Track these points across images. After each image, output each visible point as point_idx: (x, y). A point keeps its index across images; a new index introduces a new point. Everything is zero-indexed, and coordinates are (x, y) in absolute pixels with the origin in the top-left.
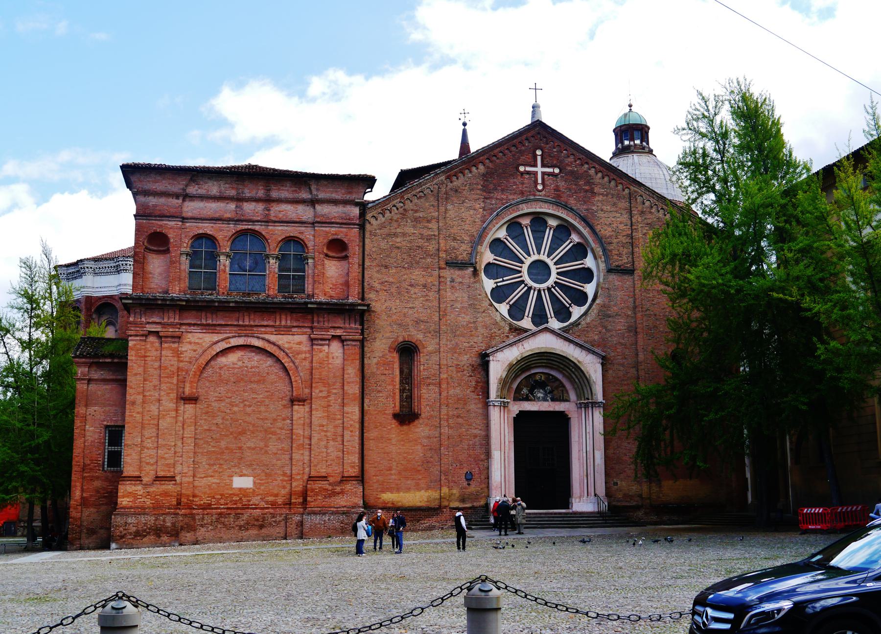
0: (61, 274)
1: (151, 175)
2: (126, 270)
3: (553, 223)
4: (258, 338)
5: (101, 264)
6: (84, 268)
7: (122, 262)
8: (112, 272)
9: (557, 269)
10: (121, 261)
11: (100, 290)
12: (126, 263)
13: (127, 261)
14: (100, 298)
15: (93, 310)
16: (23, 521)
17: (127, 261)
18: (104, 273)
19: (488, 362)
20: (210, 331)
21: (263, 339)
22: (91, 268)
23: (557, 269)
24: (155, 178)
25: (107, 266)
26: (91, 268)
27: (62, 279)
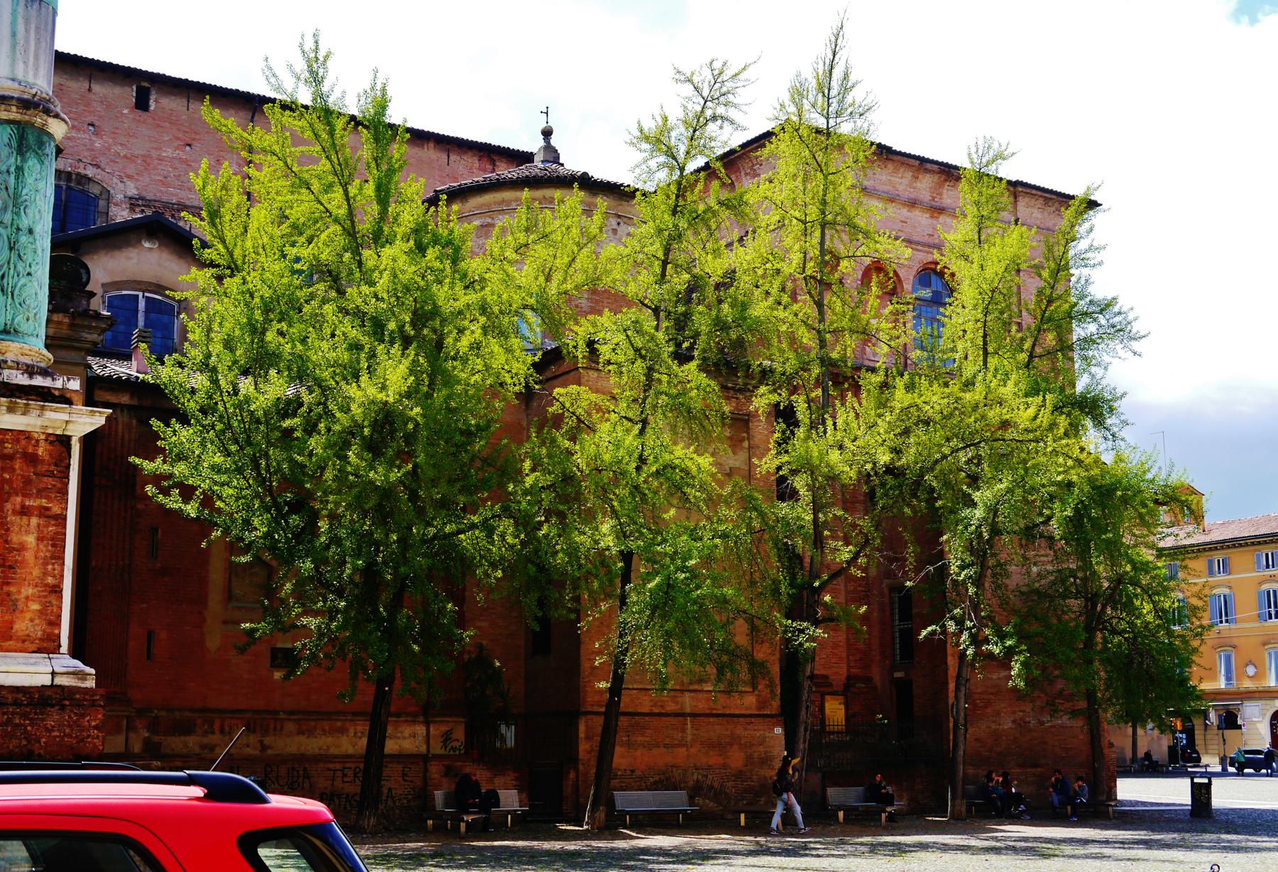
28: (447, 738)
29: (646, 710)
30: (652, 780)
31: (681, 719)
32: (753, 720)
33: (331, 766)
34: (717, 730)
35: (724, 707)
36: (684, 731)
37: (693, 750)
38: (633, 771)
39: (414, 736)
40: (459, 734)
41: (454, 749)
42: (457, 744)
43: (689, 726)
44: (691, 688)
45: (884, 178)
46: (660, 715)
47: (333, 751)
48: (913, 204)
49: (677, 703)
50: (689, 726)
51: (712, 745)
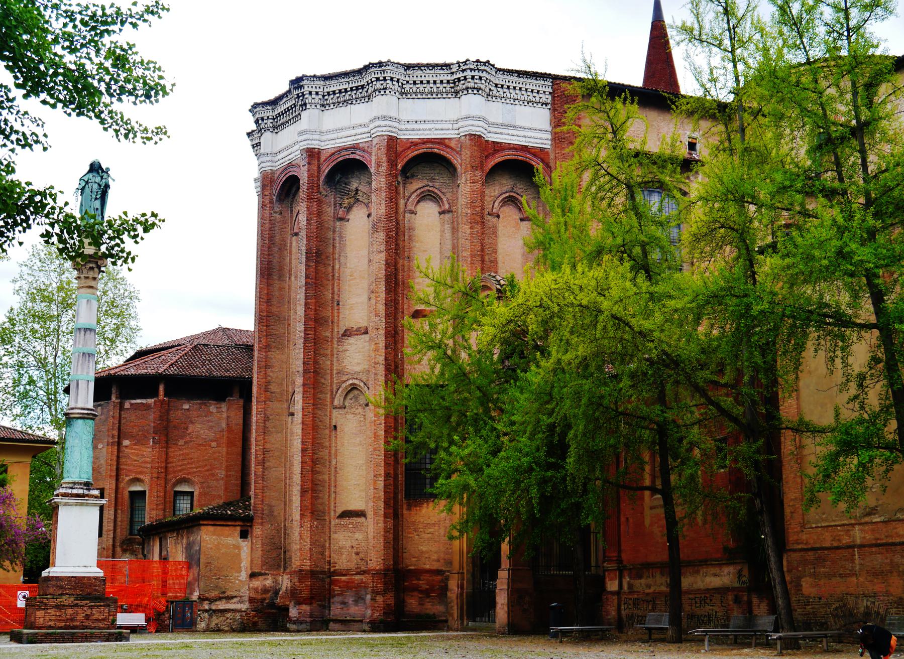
0: (310, 93)
2: (478, 89)
5: (418, 75)
6: (385, 79)
7: (473, 73)
8: (442, 93)
10: (471, 70)
11: (416, 126)
12: (480, 74)
13: (483, 71)
14: (414, 144)
15: (399, 167)
16: (207, 599)
17: (483, 71)
22: (398, 81)
25: (431, 79)
27: (311, 104)
28: (740, 574)
29: (828, 545)
30: (834, 606)
31: (850, 550)
33: (690, 596)
34: (878, 559)
35: (887, 537)
36: (853, 561)
37: (861, 579)
38: (820, 598)
39: (729, 574)
40: (745, 572)
41: (743, 583)
42: (744, 579)
43: (857, 557)
44: (863, 521)
46: (838, 548)
47: (695, 587)
49: (849, 536)
50: (857, 557)
51: (876, 574)
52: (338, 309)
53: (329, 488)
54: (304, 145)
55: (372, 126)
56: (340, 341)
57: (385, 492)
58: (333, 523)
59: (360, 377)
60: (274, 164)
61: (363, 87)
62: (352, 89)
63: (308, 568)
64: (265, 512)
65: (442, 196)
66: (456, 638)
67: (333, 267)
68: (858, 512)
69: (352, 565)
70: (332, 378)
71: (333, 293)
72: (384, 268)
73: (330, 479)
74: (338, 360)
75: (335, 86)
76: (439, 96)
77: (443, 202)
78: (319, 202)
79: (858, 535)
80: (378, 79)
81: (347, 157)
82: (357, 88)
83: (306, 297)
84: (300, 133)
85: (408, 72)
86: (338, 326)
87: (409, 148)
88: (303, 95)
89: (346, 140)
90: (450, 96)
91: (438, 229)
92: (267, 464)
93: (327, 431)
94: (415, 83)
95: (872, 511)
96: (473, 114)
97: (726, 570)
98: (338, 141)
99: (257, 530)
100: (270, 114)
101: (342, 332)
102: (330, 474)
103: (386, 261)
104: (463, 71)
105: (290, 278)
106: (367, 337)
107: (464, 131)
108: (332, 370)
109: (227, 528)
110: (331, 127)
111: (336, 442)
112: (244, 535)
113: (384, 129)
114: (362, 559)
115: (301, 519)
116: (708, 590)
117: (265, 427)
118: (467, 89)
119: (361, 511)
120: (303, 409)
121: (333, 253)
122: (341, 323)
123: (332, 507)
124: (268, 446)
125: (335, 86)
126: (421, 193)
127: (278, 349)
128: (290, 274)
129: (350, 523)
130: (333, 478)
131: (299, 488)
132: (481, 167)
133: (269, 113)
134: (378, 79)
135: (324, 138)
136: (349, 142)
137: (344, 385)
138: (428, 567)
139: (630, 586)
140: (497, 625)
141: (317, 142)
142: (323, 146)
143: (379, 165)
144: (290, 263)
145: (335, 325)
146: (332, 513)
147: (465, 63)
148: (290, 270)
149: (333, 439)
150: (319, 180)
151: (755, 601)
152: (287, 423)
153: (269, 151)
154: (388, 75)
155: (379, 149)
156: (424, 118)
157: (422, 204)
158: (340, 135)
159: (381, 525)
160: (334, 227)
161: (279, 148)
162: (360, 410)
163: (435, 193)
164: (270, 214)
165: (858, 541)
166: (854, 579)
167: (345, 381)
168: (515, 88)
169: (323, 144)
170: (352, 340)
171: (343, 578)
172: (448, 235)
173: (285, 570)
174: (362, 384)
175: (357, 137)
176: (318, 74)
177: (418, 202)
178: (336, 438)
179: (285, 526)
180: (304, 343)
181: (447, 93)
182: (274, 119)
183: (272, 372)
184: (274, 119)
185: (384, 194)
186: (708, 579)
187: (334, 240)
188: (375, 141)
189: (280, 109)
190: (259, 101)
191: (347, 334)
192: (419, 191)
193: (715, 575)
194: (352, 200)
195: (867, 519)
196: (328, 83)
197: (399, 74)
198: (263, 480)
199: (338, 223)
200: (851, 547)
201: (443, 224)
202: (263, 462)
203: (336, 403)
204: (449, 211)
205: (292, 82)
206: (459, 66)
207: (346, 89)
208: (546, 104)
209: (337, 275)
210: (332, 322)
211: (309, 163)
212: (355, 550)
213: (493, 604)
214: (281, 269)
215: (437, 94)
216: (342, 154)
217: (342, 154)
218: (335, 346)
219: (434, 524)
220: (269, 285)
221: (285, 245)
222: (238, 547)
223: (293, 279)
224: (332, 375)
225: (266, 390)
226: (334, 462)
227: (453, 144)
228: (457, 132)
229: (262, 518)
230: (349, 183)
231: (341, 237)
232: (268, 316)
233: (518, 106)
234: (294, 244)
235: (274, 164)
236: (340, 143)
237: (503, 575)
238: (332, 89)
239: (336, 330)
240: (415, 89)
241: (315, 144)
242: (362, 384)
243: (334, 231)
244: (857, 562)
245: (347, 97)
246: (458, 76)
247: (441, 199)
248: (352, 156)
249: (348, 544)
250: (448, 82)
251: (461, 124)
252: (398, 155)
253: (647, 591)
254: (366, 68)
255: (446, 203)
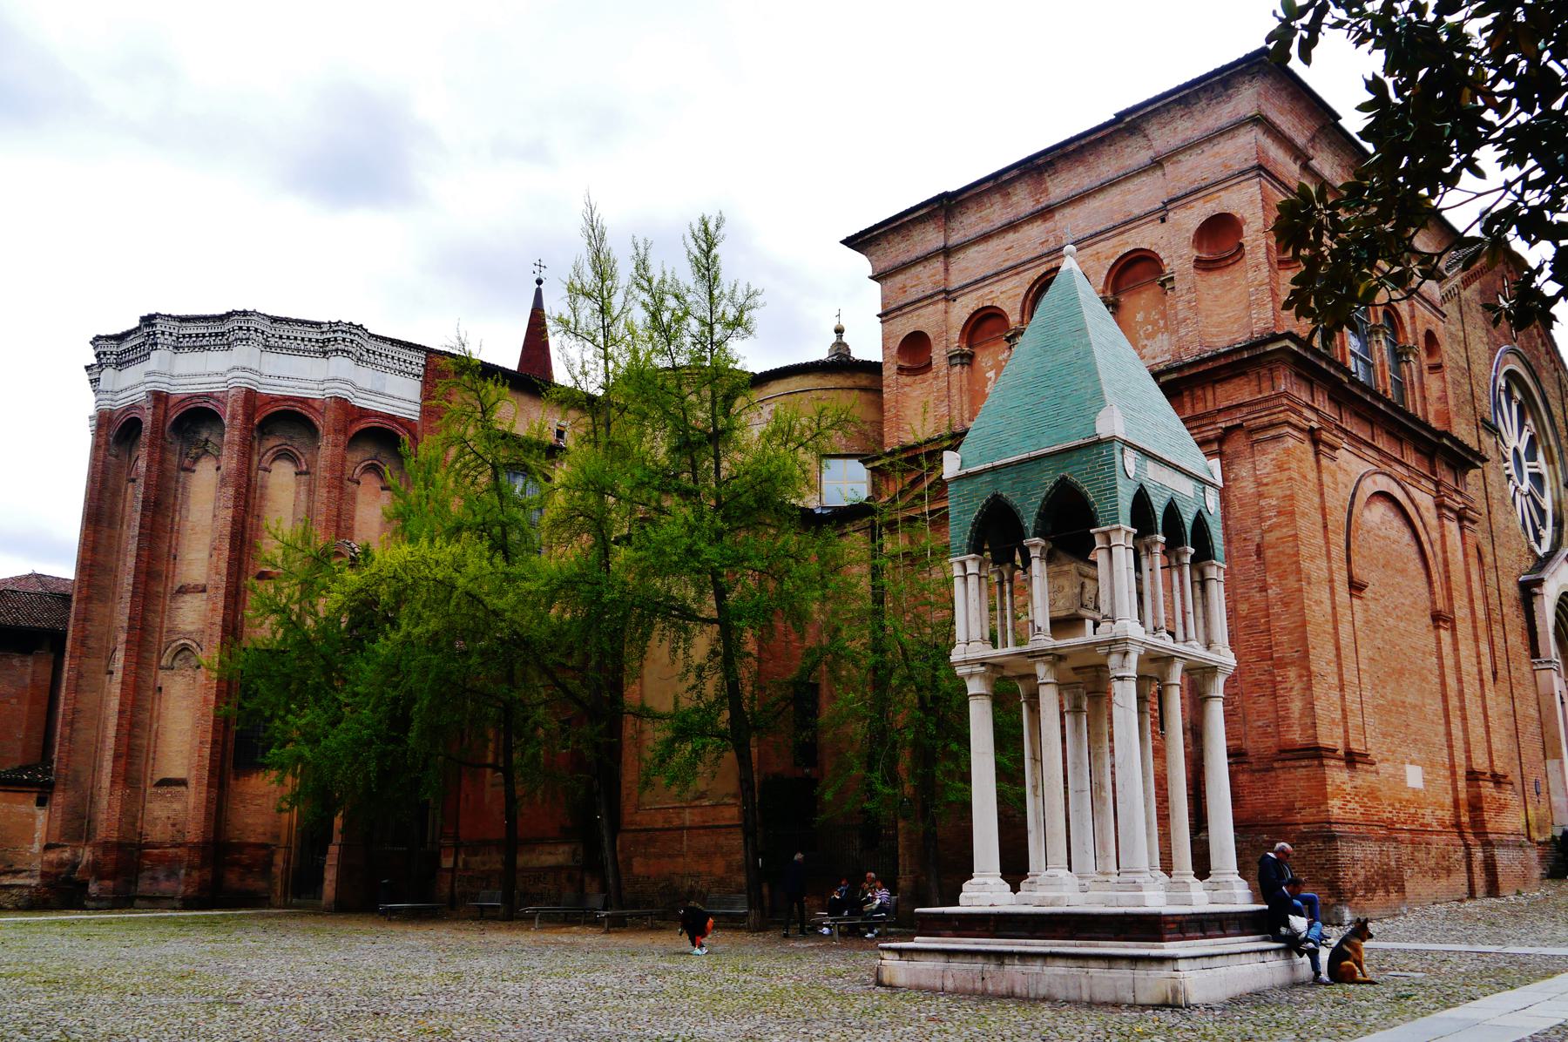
0: (163, 333)
1: (1283, 93)
2: (348, 352)
3: (1517, 394)
4: (1399, 484)
5: (285, 330)
6: (248, 329)
7: (344, 335)
8: (309, 351)
9: (1529, 467)
10: (343, 332)
11: (278, 382)
12: (352, 337)
13: (355, 334)
15: (256, 421)
17: (355, 334)
18: (288, 349)
19: (1536, 594)
20: (1356, 451)
21: (1403, 488)
22: (263, 333)
23: (1529, 467)
24: (1283, 103)
26: (263, 333)
27: (163, 344)
28: (574, 853)
29: (659, 825)
30: (661, 885)
32: (732, 830)
33: (525, 874)
37: (688, 860)
38: (649, 878)
39: (564, 853)
41: (577, 862)
44: (693, 804)
45: (973, 219)
46: (669, 829)
48: (1012, 226)
49: (679, 818)
52: (175, 564)
53: (148, 755)
54: (150, 386)
55: (229, 376)
56: (173, 598)
57: (211, 760)
58: (148, 791)
59: (194, 636)
60: (113, 403)
61: (223, 334)
62: (210, 335)
63: (115, 840)
64: (70, 778)
65: (301, 457)
66: (277, 916)
67: (173, 519)
68: (689, 796)
69: (167, 837)
70: (161, 636)
71: (170, 547)
72: (230, 525)
73: (149, 744)
74: (170, 617)
75: (191, 329)
76: (306, 354)
77: (300, 463)
78: (163, 449)
79: (688, 817)
80: (240, 328)
81: (199, 405)
82: (217, 335)
83: (139, 548)
84: (148, 374)
85: (275, 325)
86: (173, 583)
87: (269, 403)
88: (155, 334)
89: (199, 387)
90: (317, 355)
91: (293, 490)
92: (76, 726)
93: (151, 693)
94: (281, 337)
95: (702, 796)
96: (341, 376)
97: (562, 849)
98: (190, 387)
99: (58, 798)
100: (114, 349)
101: (176, 588)
102: (149, 739)
103: (233, 517)
104: (334, 332)
105: (121, 526)
106: (204, 596)
107: (329, 393)
108: (161, 628)
109: (22, 794)
110: (184, 372)
111: (159, 705)
112: (41, 802)
113: (244, 381)
114: (178, 831)
115: (111, 786)
116: (542, 868)
117: (77, 685)
118: (337, 350)
119: (180, 779)
120: (124, 667)
121: (174, 504)
122: (177, 579)
123: (149, 775)
124: (79, 706)
125: (191, 329)
126: (278, 451)
127: (101, 601)
128: (122, 523)
129: (168, 793)
130: (152, 743)
131: (112, 752)
132: (345, 431)
133: (112, 347)
134: (240, 328)
135: (174, 382)
136: (203, 389)
137: (174, 645)
138: (252, 840)
139: (466, 863)
140: (323, 903)
141: (166, 385)
142: (173, 390)
143: (233, 417)
144: (124, 509)
145: (170, 580)
146: (149, 781)
147: (337, 324)
148: (122, 518)
149: (157, 701)
150: (164, 425)
151: (587, 880)
152: (104, 682)
153: (109, 389)
154: (252, 325)
155: (235, 401)
156: (287, 375)
157: (277, 463)
158: (193, 381)
159: (204, 795)
160: (178, 478)
161: (122, 387)
162: (190, 672)
163: (293, 453)
164: (105, 456)
165: (688, 823)
166: (681, 860)
167: (175, 641)
168: (387, 356)
169: (173, 388)
170: (187, 597)
171: (156, 851)
172: (303, 497)
173: (87, 841)
174: (194, 645)
175: (211, 386)
176: (174, 313)
177: (274, 460)
178: (160, 699)
179: (92, 793)
180: (132, 597)
181: (315, 352)
182: (118, 355)
183: (91, 625)
184: (118, 355)
185: (236, 448)
186: (543, 858)
187: (177, 490)
188: (232, 392)
189: (126, 346)
190: (103, 334)
191: (183, 590)
192: (275, 449)
193: (550, 853)
194: (200, 451)
195: (697, 803)
196: (184, 324)
197: (264, 326)
198: (70, 741)
199: (182, 473)
200: (680, 829)
201: (298, 486)
202: (72, 723)
203: (163, 663)
204: (307, 473)
205: (143, 319)
206: (331, 327)
207: (204, 334)
208: (418, 376)
209: (176, 527)
210: (167, 577)
211: (154, 407)
212: (171, 821)
213: (321, 880)
214: (112, 515)
215: (304, 351)
216: (194, 401)
217: (194, 401)
218: (168, 602)
219: (263, 796)
220: (96, 532)
221: (120, 490)
222: (33, 816)
223: (125, 527)
224: (161, 633)
225: (83, 644)
226: (155, 726)
227: (316, 405)
228: (322, 393)
229: (65, 785)
230: (198, 433)
231: (184, 488)
232: (91, 565)
233: (388, 375)
234: (130, 490)
235: (113, 403)
236: (192, 390)
237: (333, 850)
238: (188, 332)
239: (170, 585)
240: (280, 343)
241: (164, 388)
242: (194, 645)
243: (177, 482)
244: (685, 843)
245: (205, 342)
246: (328, 336)
247: (299, 460)
248: (205, 405)
249: (164, 815)
250: (317, 341)
251: (326, 385)
252: (255, 409)
253: (482, 868)
254: (229, 315)
255: (304, 464)
